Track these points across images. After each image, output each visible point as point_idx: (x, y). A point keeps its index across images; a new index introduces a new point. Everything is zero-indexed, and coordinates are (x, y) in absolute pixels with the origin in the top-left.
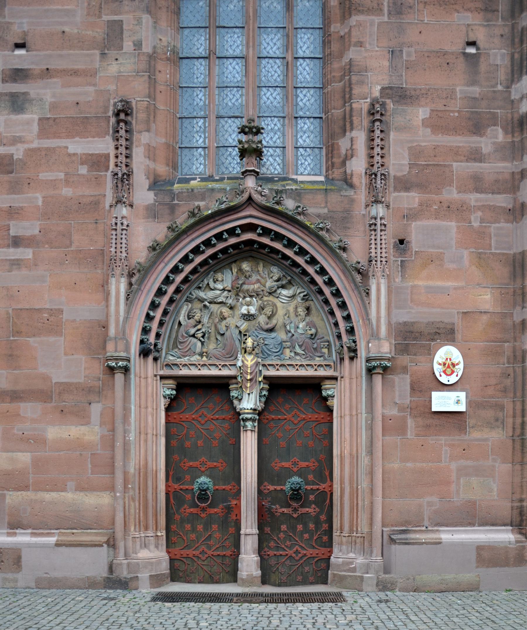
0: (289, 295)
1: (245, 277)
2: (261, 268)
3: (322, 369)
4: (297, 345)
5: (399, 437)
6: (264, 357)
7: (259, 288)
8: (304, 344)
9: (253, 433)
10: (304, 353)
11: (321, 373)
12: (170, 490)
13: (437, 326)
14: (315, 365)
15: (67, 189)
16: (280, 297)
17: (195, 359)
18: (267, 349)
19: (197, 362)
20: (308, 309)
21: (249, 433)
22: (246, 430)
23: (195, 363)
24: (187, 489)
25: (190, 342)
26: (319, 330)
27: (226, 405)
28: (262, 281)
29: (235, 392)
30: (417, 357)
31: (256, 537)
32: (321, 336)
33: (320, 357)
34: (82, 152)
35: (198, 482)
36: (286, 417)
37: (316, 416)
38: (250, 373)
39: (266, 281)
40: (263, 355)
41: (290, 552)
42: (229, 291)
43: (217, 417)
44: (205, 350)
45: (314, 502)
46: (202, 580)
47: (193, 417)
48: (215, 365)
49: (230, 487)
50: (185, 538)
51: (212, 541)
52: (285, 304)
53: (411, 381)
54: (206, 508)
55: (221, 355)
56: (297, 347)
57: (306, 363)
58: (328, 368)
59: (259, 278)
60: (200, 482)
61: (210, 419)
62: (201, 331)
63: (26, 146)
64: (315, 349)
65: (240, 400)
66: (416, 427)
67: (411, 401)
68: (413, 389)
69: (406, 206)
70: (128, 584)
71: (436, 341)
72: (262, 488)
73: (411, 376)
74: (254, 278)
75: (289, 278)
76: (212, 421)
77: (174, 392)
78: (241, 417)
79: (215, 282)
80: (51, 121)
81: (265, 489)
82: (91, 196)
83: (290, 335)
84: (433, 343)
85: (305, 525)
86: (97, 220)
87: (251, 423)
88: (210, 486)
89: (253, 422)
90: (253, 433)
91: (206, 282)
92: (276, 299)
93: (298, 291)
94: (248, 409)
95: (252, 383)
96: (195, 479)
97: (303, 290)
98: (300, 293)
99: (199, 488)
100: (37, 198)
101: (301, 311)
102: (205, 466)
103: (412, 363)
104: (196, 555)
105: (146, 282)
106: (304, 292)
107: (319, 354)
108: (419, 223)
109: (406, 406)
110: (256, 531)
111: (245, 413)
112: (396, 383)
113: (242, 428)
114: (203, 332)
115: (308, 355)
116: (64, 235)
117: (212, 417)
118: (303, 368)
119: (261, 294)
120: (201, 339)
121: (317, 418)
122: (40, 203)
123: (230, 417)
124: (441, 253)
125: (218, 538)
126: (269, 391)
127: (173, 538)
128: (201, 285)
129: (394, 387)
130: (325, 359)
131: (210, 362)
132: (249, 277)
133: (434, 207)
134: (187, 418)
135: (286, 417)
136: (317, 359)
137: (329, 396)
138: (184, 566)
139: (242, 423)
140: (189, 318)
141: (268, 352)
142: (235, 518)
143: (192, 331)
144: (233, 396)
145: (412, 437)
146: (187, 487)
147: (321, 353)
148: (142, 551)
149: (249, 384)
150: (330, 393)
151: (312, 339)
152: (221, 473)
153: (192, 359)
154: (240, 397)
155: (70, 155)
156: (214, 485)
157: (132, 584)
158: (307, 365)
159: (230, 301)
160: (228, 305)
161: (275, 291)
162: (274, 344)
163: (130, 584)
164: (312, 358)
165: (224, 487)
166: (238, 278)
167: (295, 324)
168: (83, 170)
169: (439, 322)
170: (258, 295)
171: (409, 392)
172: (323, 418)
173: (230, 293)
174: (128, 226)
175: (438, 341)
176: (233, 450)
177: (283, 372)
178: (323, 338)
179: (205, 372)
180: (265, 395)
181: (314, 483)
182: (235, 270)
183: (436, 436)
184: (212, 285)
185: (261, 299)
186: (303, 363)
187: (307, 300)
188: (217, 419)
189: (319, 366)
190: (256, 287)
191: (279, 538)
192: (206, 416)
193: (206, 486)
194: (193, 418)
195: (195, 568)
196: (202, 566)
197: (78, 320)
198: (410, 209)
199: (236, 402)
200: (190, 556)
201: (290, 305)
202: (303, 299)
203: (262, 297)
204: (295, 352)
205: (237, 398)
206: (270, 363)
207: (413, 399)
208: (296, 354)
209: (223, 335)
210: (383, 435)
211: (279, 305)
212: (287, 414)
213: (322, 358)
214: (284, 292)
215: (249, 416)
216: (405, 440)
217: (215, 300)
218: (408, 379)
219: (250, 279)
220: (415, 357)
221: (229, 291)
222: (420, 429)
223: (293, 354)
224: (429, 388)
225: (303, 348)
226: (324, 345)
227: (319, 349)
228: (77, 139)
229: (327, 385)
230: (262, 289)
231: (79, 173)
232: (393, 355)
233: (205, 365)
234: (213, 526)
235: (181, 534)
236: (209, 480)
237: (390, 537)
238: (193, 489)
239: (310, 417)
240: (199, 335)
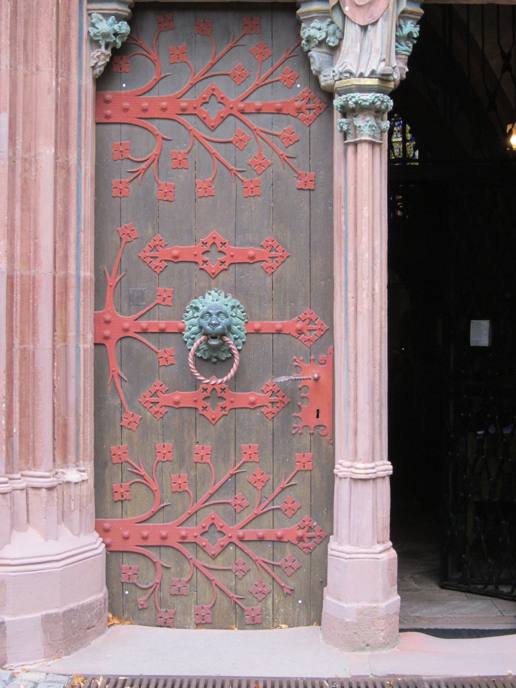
9: (377, 149)
12: (107, 333)
21: (364, 151)
22: (355, 144)
27: (288, 66)
29: (316, 24)
31: (385, 488)
35: (197, 309)
43: (258, 104)
46: (208, 619)
47: (184, 104)
49: (299, 326)
54: (223, 390)
60: (203, 309)
61: (235, 112)
65: (334, 50)
77: (124, 28)
78: (337, 102)
87: (370, 120)
88: (235, 320)
89: (376, 117)
90: (377, 149)
94: (361, 75)
96: (189, 299)
99: (201, 328)
102: (222, 257)
104: (191, 539)
111: (349, 90)
113: (337, 136)
123: (298, 104)
134: (164, 109)
138: (151, 573)
139: (339, 120)
142: (313, 421)
144: (309, 40)
148: (18, 537)
154: (332, 41)
176: (306, 208)
180: (410, 36)
192: (222, 101)
193: (224, 321)
194: (184, 110)
195: (185, 579)
205: (322, 43)
215: (368, 97)
234: (244, 446)
236: (232, 301)
238: (181, 332)
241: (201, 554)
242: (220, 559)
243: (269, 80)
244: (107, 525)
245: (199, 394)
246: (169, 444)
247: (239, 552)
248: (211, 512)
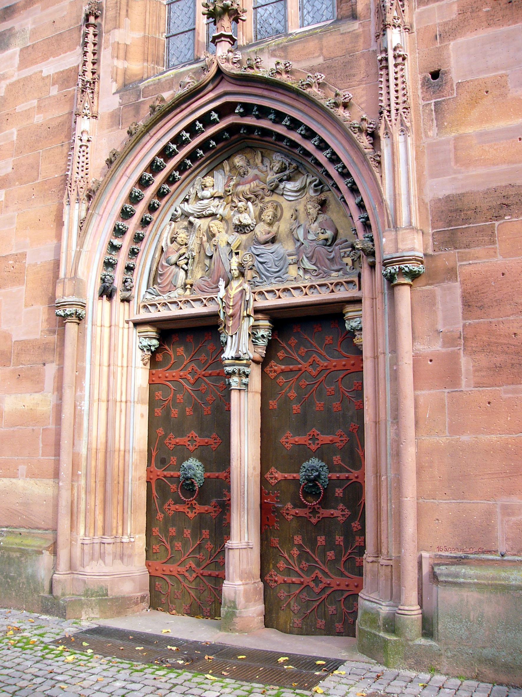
0: (295, 189)
1: (239, 174)
3: (342, 288)
4: (304, 256)
5: (447, 390)
6: (261, 281)
7: (257, 186)
8: (315, 255)
10: (315, 268)
11: (341, 294)
13: (504, 194)
14: (332, 284)
15: (39, 116)
16: (285, 193)
18: (265, 268)
19: (179, 298)
23: (175, 300)
24: (172, 477)
25: (170, 274)
26: (341, 231)
28: (261, 175)
30: (472, 250)
32: (344, 239)
33: (338, 271)
34: (54, 72)
36: (300, 366)
37: (344, 363)
38: (232, 306)
40: (262, 278)
43: (210, 372)
44: (189, 281)
45: (343, 500)
47: (181, 374)
48: (199, 300)
50: (169, 547)
51: (201, 554)
52: (292, 202)
53: (463, 292)
55: (207, 285)
57: (318, 283)
58: (351, 286)
59: (259, 173)
62: (184, 257)
63: (8, 82)
64: (332, 260)
66: (476, 371)
67: (464, 326)
68: (467, 304)
69: (438, 21)
71: (503, 218)
72: (268, 475)
73: (462, 283)
74: (252, 172)
76: (205, 378)
80: (30, 49)
81: (272, 478)
82: (60, 117)
83: (299, 244)
84: (497, 223)
85: (330, 536)
86: (63, 142)
92: (281, 197)
93: (308, 181)
94: (228, 359)
95: (234, 320)
97: (314, 178)
98: (311, 183)
100: (13, 133)
103: (462, 261)
105: (105, 204)
106: (315, 180)
107: (339, 267)
108: (460, 40)
109: (457, 335)
112: (439, 298)
114: (186, 258)
115: (321, 271)
116: (33, 168)
117: (203, 373)
118: (315, 291)
119: (260, 195)
120: (185, 266)
121: (344, 365)
122: (15, 138)
124: (501, 76)
125: (209, 550)
126: (274, 330)
127: (154, 547)
128: (187, 197)
129: (434, 305)
130: (345, 274)
131: (194, 297)
132: (244, 174)
133: (484, 10)
135: (300, 366)
136: (334, 274)
137: (354, 329)
140: (172, 242)
141: (267, 273)
143: (173, 258)
145: (468, 389)
146: (172, 473)
147: (341, 264)
149: (231, 322)
150: (354, 324)
151: (330, 246)
152: (214, 453)
153: (172, 295)
155: (43, 79)
156: (206, 470)
158: (319, 285)
160: (218, 216)
161: (277, 187)
162: (274, 261)
164: (327, 275)
165: (217, 474)
167: (305, 229)
168: (54, 91)
169: (506, 187)
170: (256, 196)
171: (460, 311)
172: (353, 365)
173: (222, 201)
174: (88, 141)
175: (506, 218)
177: (286, 300)
178: (346, 241)
179: (187, 311)
181: (342, 470)
182: (227, 168)
183: (513, 384)
185: (261, 202)
186: (314, 284)
187: (322, 191)
188: (210, 375)
189: (337, 284)
190: (252, 186)
196: (188, 589)
197: (39, 263)
198: (446, 24)
200: (175, 573)
201: (300, 203)
202: (316, 191)
203: (262, 198)
204: (304, 269)
206: (269, 288)
207: (468, 322)
208: (306, 271)
209: (211, 257)
210: (415, 389)
211: (285, 204)
212: (302, 362)
213: (341, 273)
214: (290, 186)
216: (457, 393)
217: (204, 213)
218: (457, 288)
219: (246, 176)
220: (467, 250)
221: (220, 198)
222: (484, 374)
223: (301, 273)
224: (496, 301)
225: (314, 261)
226: (345, 253)
227: (338, 260)
228: (51, 59)
229: (350, 311)
230: (261, 187)
231: (50, 95)
232: (430, 251)
233: (188, 301)
235: (164, 541)
237: (433, 568)
239: (334, 364)
240: (182, 262)
241: (186, 581)
242: (194, 583)
243: (215, 360)
244: (150, 564)
245: (307, 510)
247: (201, 581)
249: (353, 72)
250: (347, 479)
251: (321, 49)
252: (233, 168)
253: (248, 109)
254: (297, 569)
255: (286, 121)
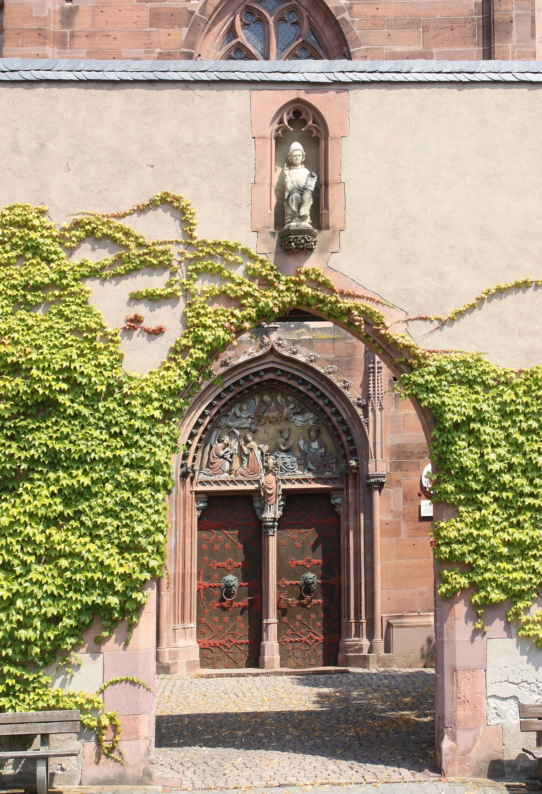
2: (279, 398)
17: (225, 476)
20: (318, 432)
39: (284, 408)
40: (281, 471)
41: (304, 638)
42: (253, 418)
56: (310, 463)
70: (169, 669)
75: (303, 406)
78: (263, 524)
79: (241, 411)
91: (233, 411)
101: (313, 434)
110: (277, 621)
143: (222, 453)
157: (172, 669)
159: (253, 427)
163: (171, 668)
166: (259, 407)
182: (257, 400)
184: (238, 413)
191: (295, 626)
199: (258, 511)
221: (253, 418)
225: (315, 464)
240: (228, 456)
246: (217, 618)
248: (229, 636)
249: (351, 367)
250: (328, 583)
251: (334, 349)
252: (262, 400)
253: (284, 373)
254: (299, 633)
255: (309, 387)
